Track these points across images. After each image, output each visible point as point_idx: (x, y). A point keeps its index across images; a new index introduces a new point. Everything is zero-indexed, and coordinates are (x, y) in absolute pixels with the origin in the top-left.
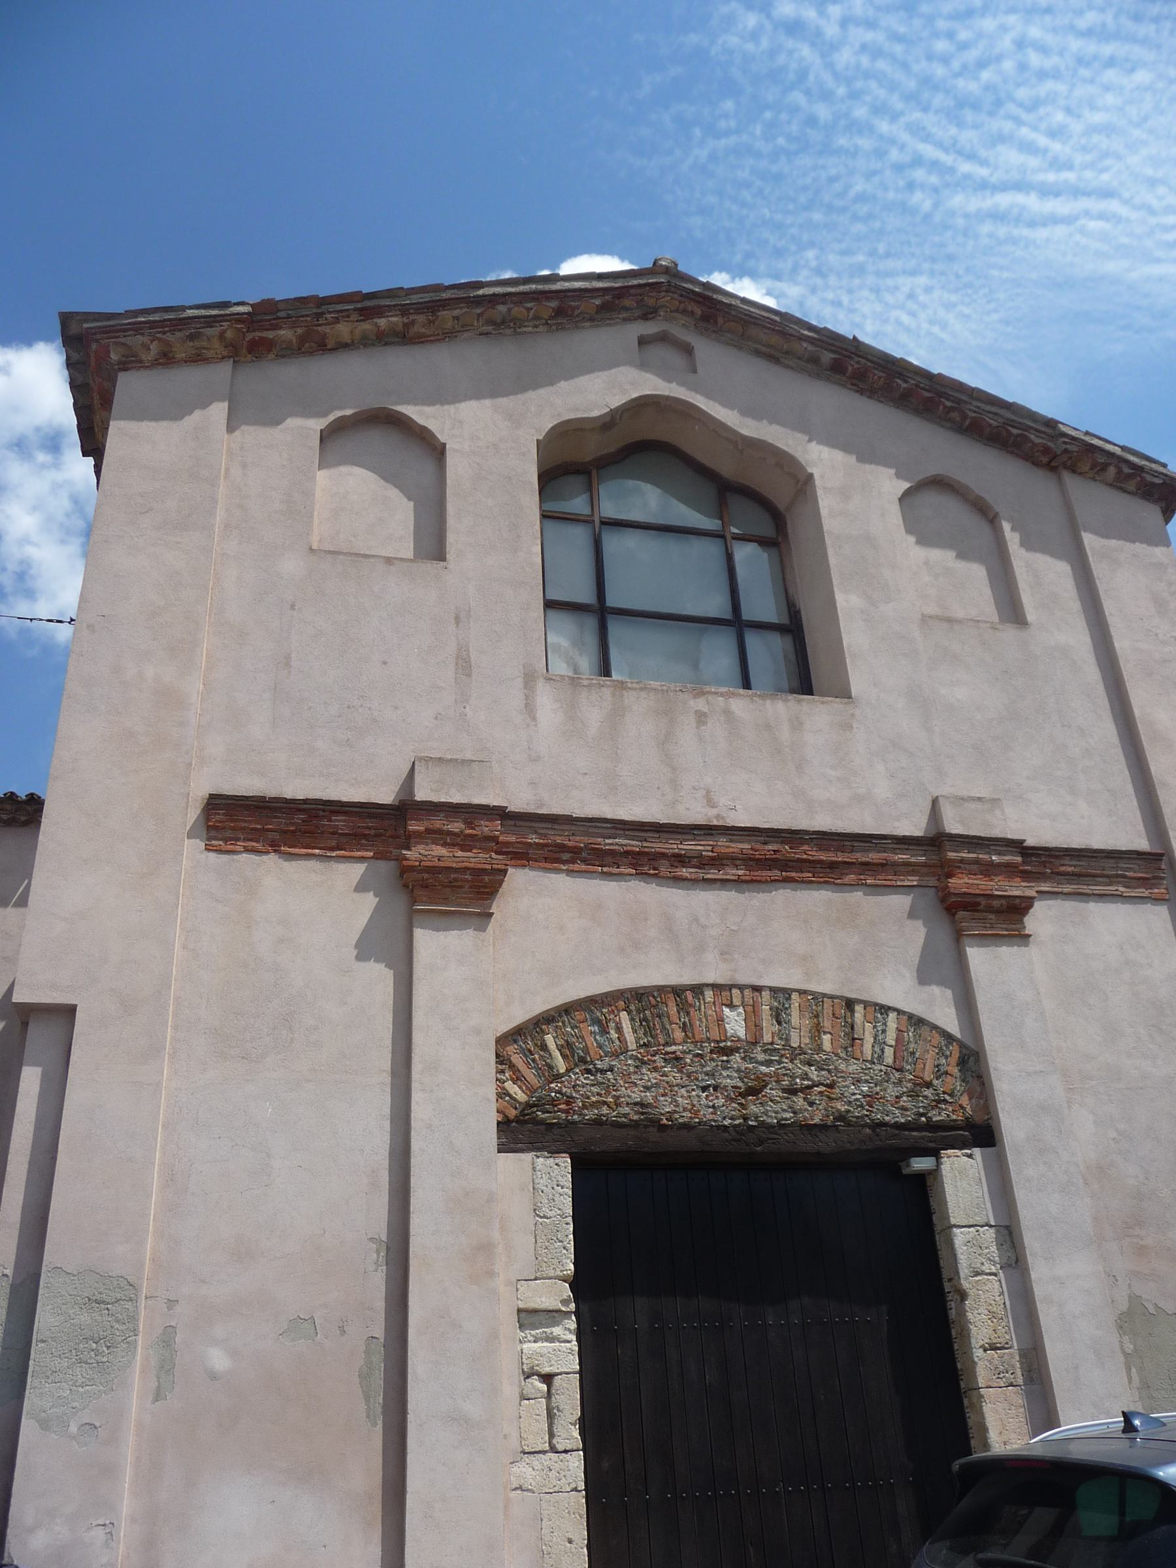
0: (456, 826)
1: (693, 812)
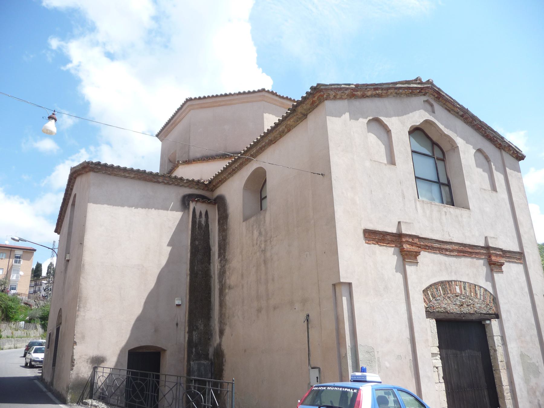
0: (410, 240)
1: (446, 238)
